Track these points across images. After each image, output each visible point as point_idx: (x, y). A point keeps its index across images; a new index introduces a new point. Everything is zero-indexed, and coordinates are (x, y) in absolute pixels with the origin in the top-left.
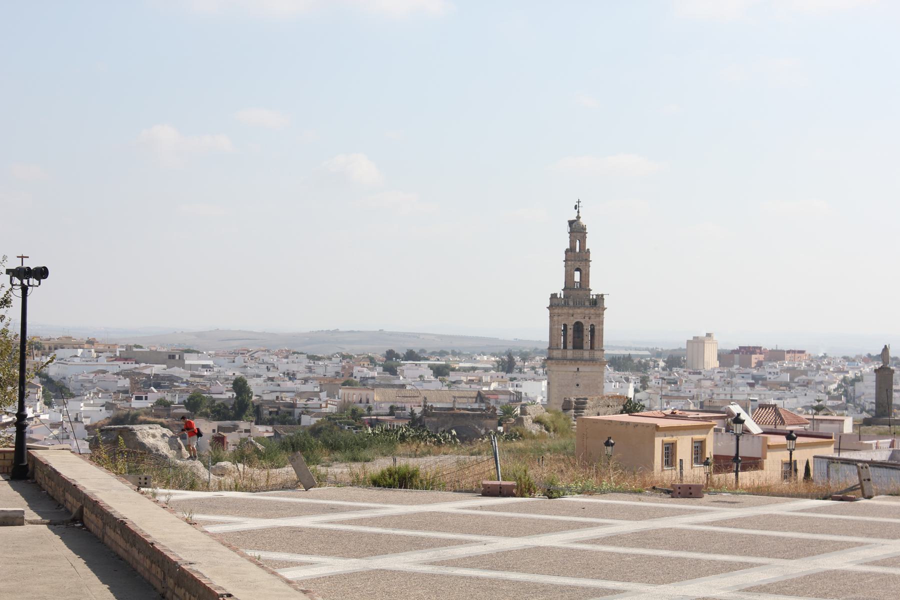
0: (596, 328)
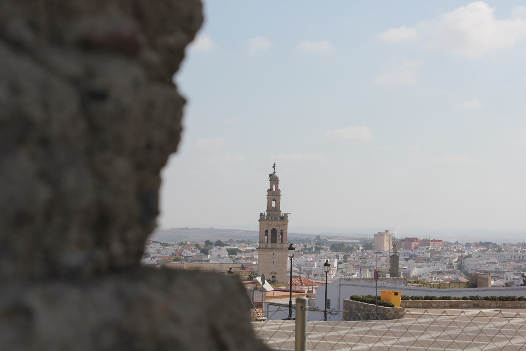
0: (284, 232)
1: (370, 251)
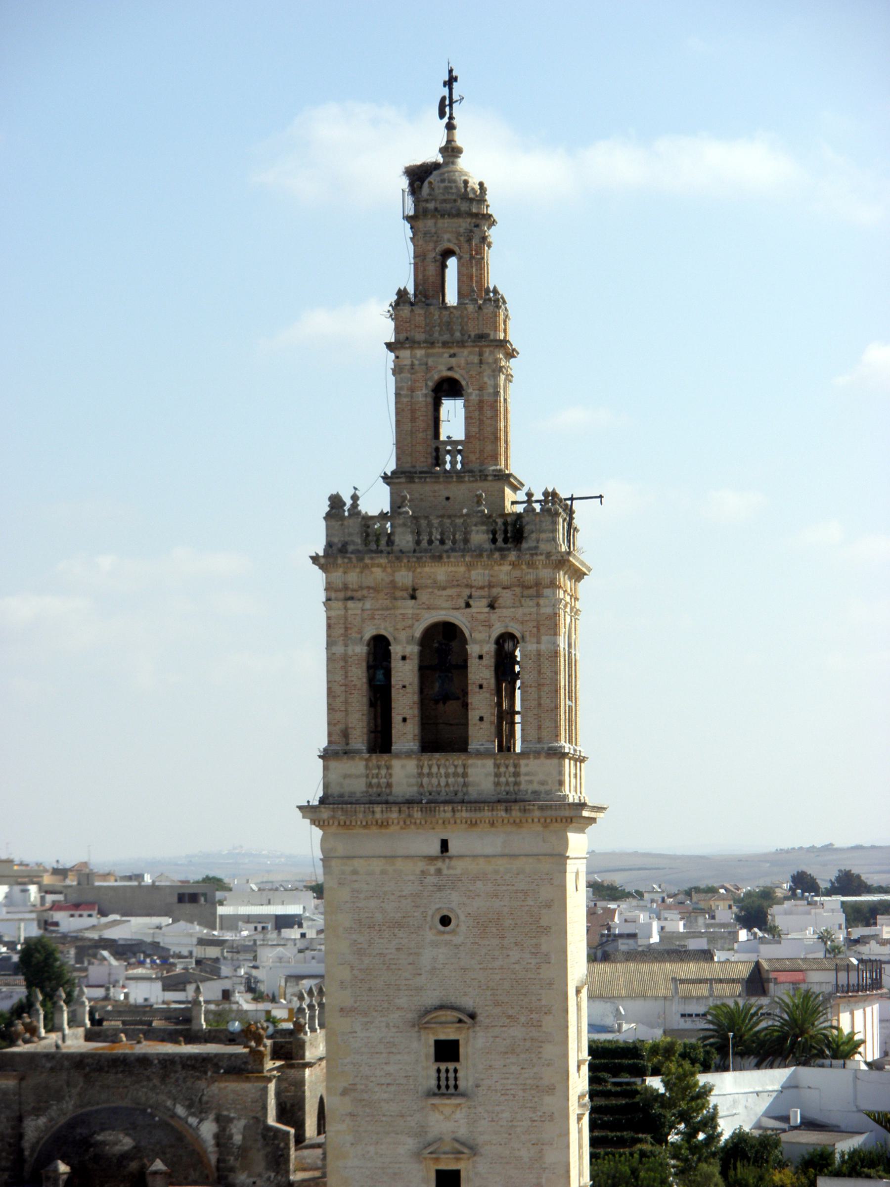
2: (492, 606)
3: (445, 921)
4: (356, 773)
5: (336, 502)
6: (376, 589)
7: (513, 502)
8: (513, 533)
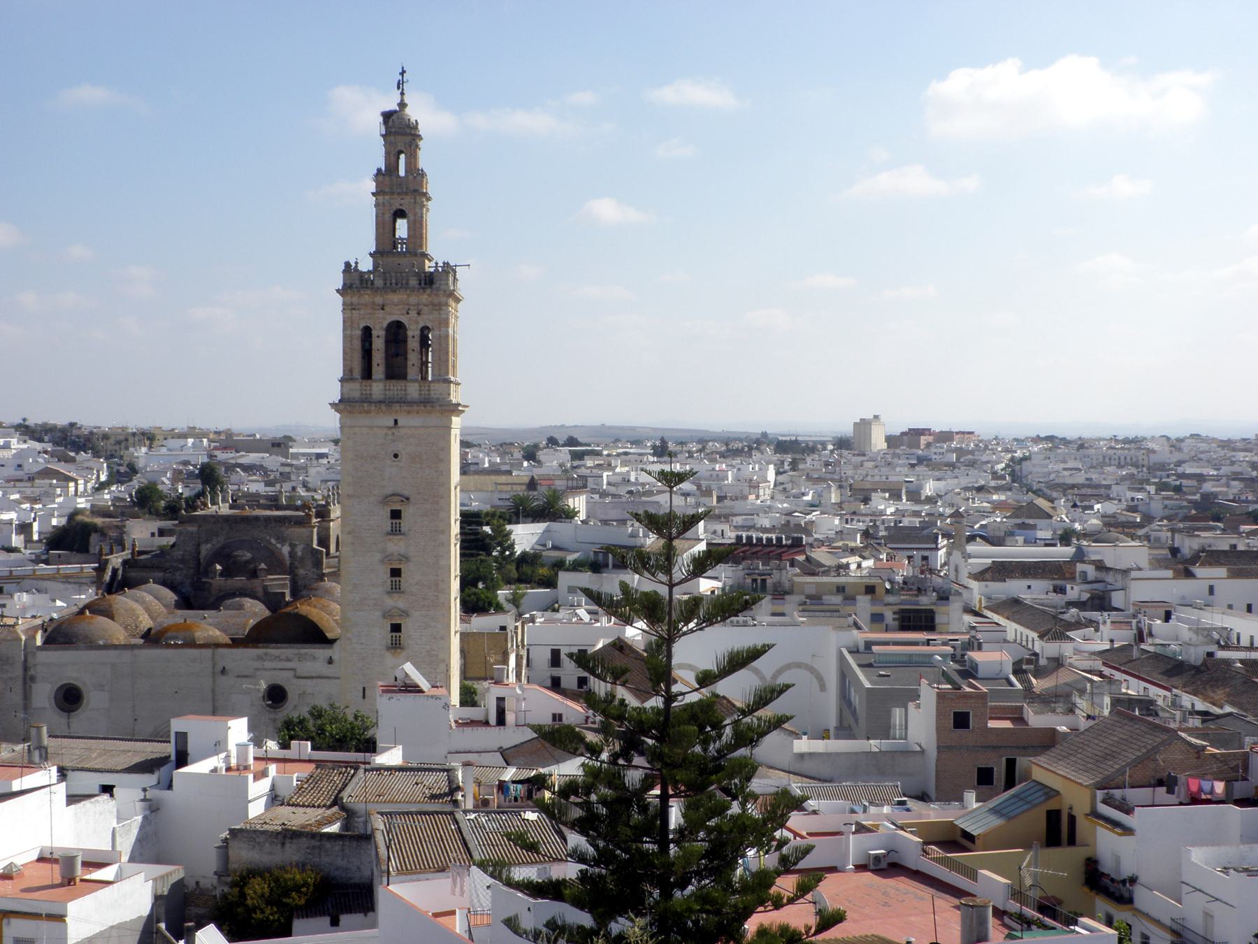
1: (845, 453)
2: (419, 314)
3: (396, 456)
4: (356, 389)
5: (348, 265)
6: (366, 305)
7: (429, 267)
8: (429, 281)
